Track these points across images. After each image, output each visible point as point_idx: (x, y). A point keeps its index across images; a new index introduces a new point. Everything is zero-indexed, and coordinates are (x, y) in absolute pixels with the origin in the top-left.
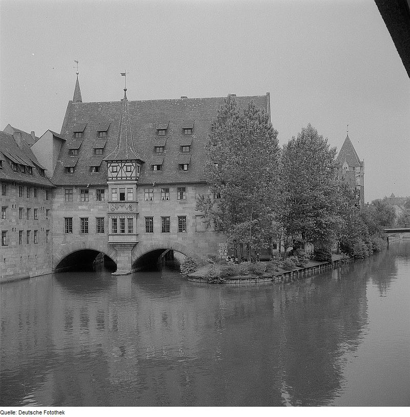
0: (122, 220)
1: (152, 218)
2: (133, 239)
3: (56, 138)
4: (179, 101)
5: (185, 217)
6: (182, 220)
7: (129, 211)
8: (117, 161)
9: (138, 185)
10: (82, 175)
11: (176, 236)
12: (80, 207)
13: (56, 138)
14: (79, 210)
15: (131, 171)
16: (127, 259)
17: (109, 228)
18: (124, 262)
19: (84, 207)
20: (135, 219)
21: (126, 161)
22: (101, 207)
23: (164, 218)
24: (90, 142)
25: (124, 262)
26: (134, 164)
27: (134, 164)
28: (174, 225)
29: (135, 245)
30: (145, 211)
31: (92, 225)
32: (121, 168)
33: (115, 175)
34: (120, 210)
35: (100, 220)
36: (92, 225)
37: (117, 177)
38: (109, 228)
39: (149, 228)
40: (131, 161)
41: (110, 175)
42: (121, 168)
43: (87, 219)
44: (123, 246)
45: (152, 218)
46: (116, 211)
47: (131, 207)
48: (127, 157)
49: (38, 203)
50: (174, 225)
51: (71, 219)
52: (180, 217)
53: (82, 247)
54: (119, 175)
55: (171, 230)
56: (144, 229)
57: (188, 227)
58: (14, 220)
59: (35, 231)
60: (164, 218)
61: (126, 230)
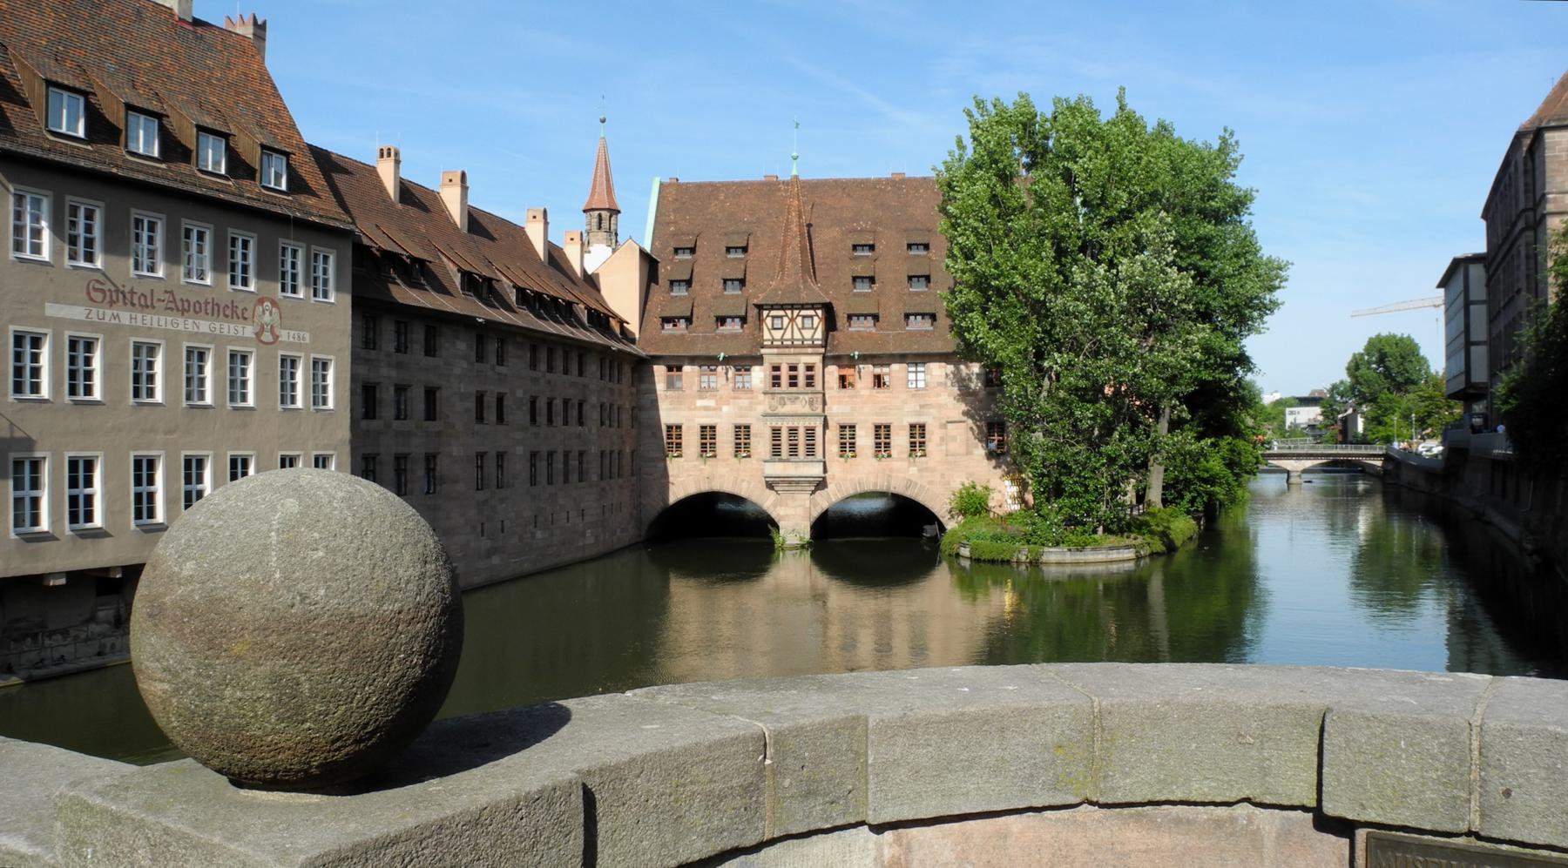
0: (793, 431)
1: (852, 427)
2: (815, 470)
3: (643, 253)
4: (889, 182)
5: (922, 427)
6: (918, 433)
7: (807, 410)
8: (782, 307)
9: (826, 360)
10: (701, 337)
11: (905, 464)
12: (699, 403)
13: (643, 253)
14: (696, 409)
15: (811, 328)
16: (800, 511)
17: (761, 444)
18: (794, 518)
19: (711, 403)
20: (819, 431)
21: (803, 307)
22: (745, 402)
23: (878, 427)
24: (711, 266)
25: (794, 518)
26: (819, 312)
27: (819, 312)
28: (900, 440)
29: (821, 484)
30: (841, 407)
31: (725, 440)
32: (792, 320)
33: (777, 334)
34: (789, 408)
35: (742, 433)
36: (725, 440)
37: (782, 340)
38: (761, 444)
39: (848, 445)
40: (813, 306)
41: (766, 335)
42: (792, 320)
43: (713, 428)
44: (791, 482)
45: (852, 427)
46: (781, 410)
47: (811, 403)
48: (804, 298)
49: (620, 392)
50: (900, 440)
51: (679, 427)
52: (913, 427)
53: (704, 488)
54: (788, 335)
55: (894, 452)
56: (833, 448)
57: (929, 447)
58: (594, 430)
59: (620, 453)
60: (878, 427)
61: (802, 449)
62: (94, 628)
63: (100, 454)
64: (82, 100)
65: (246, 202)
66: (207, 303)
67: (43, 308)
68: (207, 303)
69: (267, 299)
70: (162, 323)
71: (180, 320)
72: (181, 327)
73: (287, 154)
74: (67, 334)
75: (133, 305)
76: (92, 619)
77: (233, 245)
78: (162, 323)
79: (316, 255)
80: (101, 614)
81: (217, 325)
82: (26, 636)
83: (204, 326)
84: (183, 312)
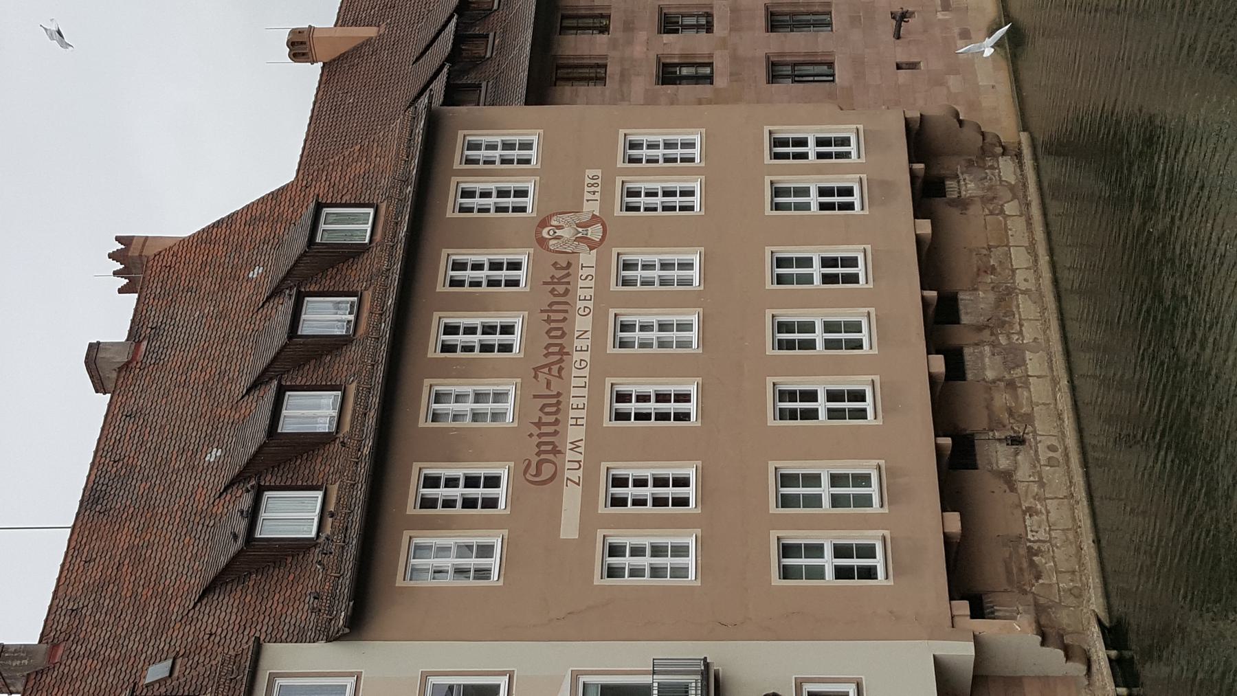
62: (1023, 473)
63: (772, 465)
64: (267, 494)
65: (398, 267)
66: (549, 321)
67: (567, 541)
68: (549, 321)
69: (538, 232)
70: (581, 382)
71: (576, 356)
72: (587, 356)
73: (319, 207)
74: (604, 509)
75: (557, 422)
76: (1007, 477)
77: (460, 283)
78: (581, 382)
79: (469, 161)
80: (1003, 464)
81: (580, 304)
82: (1032, 564)
83: (583, 323)
84: (563, 353)
